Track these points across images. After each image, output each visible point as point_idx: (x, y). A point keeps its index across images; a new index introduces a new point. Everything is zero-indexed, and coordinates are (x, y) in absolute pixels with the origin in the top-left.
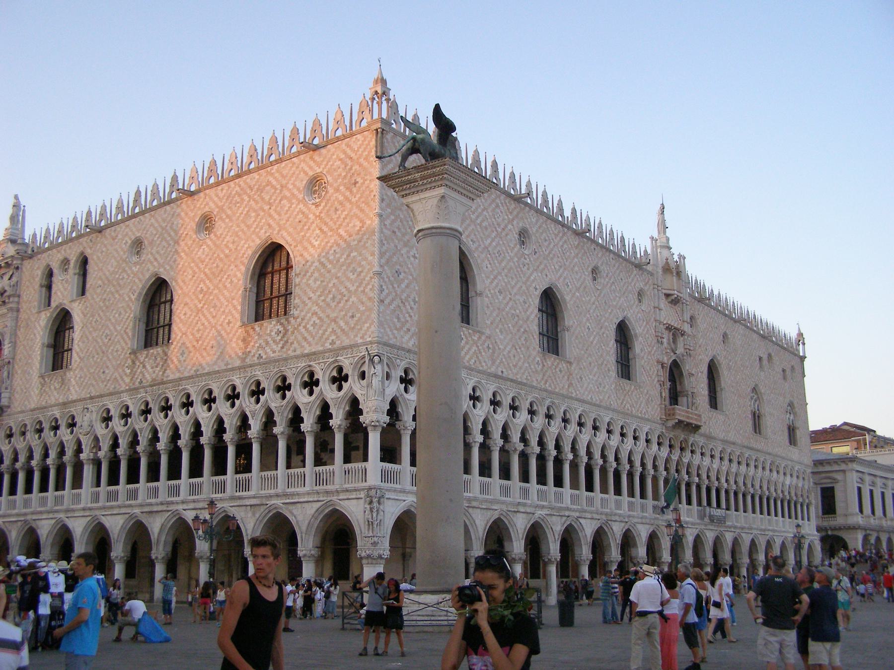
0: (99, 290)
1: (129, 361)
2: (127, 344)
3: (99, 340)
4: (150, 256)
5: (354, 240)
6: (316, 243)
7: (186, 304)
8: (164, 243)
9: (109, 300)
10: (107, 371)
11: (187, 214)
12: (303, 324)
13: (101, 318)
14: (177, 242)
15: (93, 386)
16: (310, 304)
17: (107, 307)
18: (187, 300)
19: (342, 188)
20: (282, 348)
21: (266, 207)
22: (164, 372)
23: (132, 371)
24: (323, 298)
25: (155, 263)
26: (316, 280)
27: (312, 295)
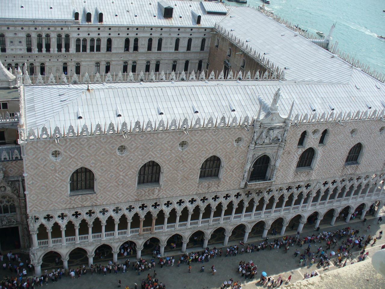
0: (333, 144)
1: (342, 168)
2: (342, 163)
3: (330, 161)
4: (359, 136)
7: (369, 153)
8: (366, 133)
9: (338, 148)
10: (331, 171)
11: (377, 125)
13: (332, 154)
14: (371, 134)
15: (324, 175)
17: (336, 151)
18: (370, 152)
25: (361, 139)
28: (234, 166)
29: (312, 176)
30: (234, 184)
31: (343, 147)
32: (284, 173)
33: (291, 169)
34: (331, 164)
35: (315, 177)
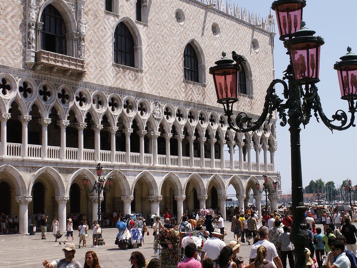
0: (157, 27)
2: (181, 73)
5: (268, 76)
6: (258, 70)
8: (196, 24)
12: (256, 103)
15: (161, 89)
16: (258, 95)
19: (264, 52)
20: (251, 109)
21: (240, 41)
22: (204, 99)
23: (185, 92)
24: (261, 95)
25: (192, 33)
26: (259, 86)
27: (258, 92)
28: (6, 7)
29: (144, 84)
30: (14, 55)
31: (173, 39)
32: (97, 59)
33: (107, 55)
34: (166, 68)
35: (148, 88)
